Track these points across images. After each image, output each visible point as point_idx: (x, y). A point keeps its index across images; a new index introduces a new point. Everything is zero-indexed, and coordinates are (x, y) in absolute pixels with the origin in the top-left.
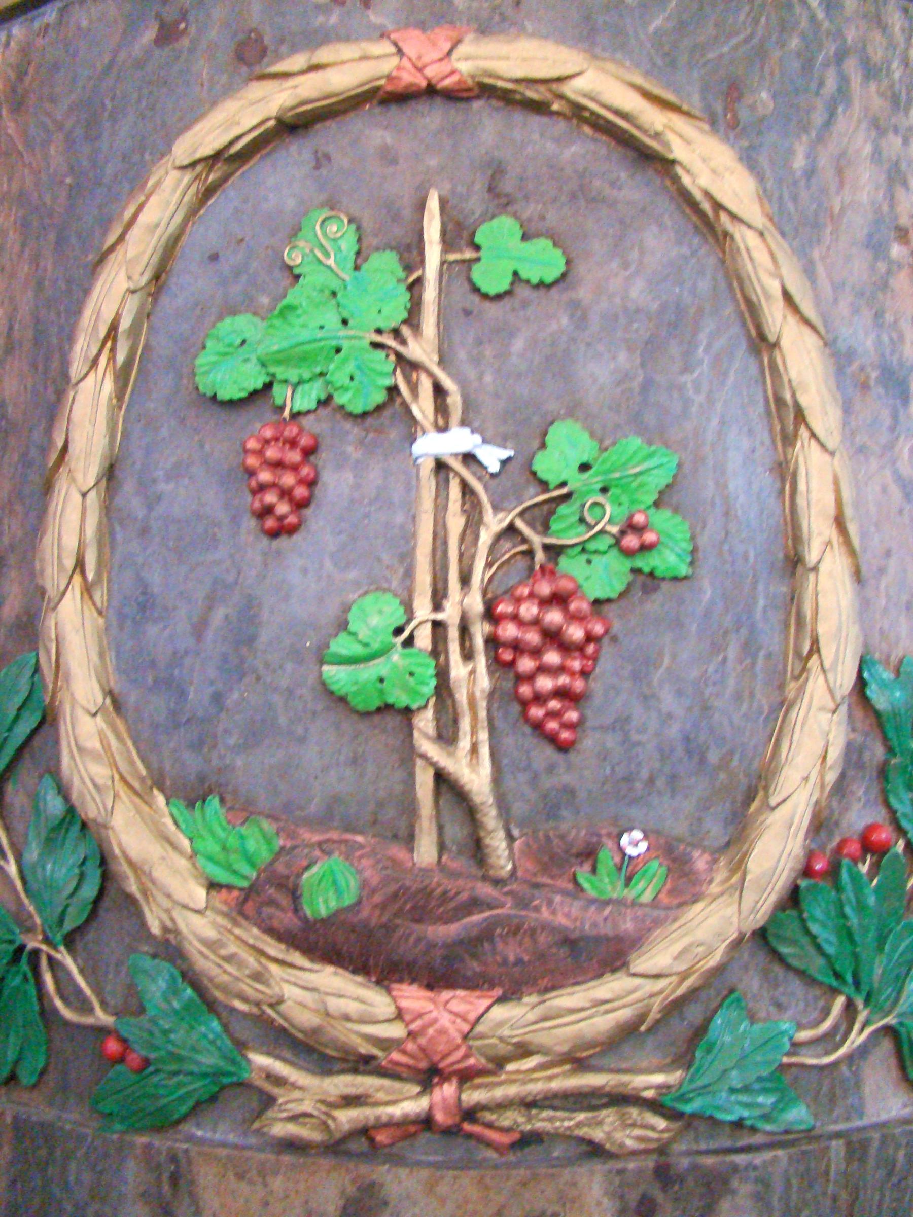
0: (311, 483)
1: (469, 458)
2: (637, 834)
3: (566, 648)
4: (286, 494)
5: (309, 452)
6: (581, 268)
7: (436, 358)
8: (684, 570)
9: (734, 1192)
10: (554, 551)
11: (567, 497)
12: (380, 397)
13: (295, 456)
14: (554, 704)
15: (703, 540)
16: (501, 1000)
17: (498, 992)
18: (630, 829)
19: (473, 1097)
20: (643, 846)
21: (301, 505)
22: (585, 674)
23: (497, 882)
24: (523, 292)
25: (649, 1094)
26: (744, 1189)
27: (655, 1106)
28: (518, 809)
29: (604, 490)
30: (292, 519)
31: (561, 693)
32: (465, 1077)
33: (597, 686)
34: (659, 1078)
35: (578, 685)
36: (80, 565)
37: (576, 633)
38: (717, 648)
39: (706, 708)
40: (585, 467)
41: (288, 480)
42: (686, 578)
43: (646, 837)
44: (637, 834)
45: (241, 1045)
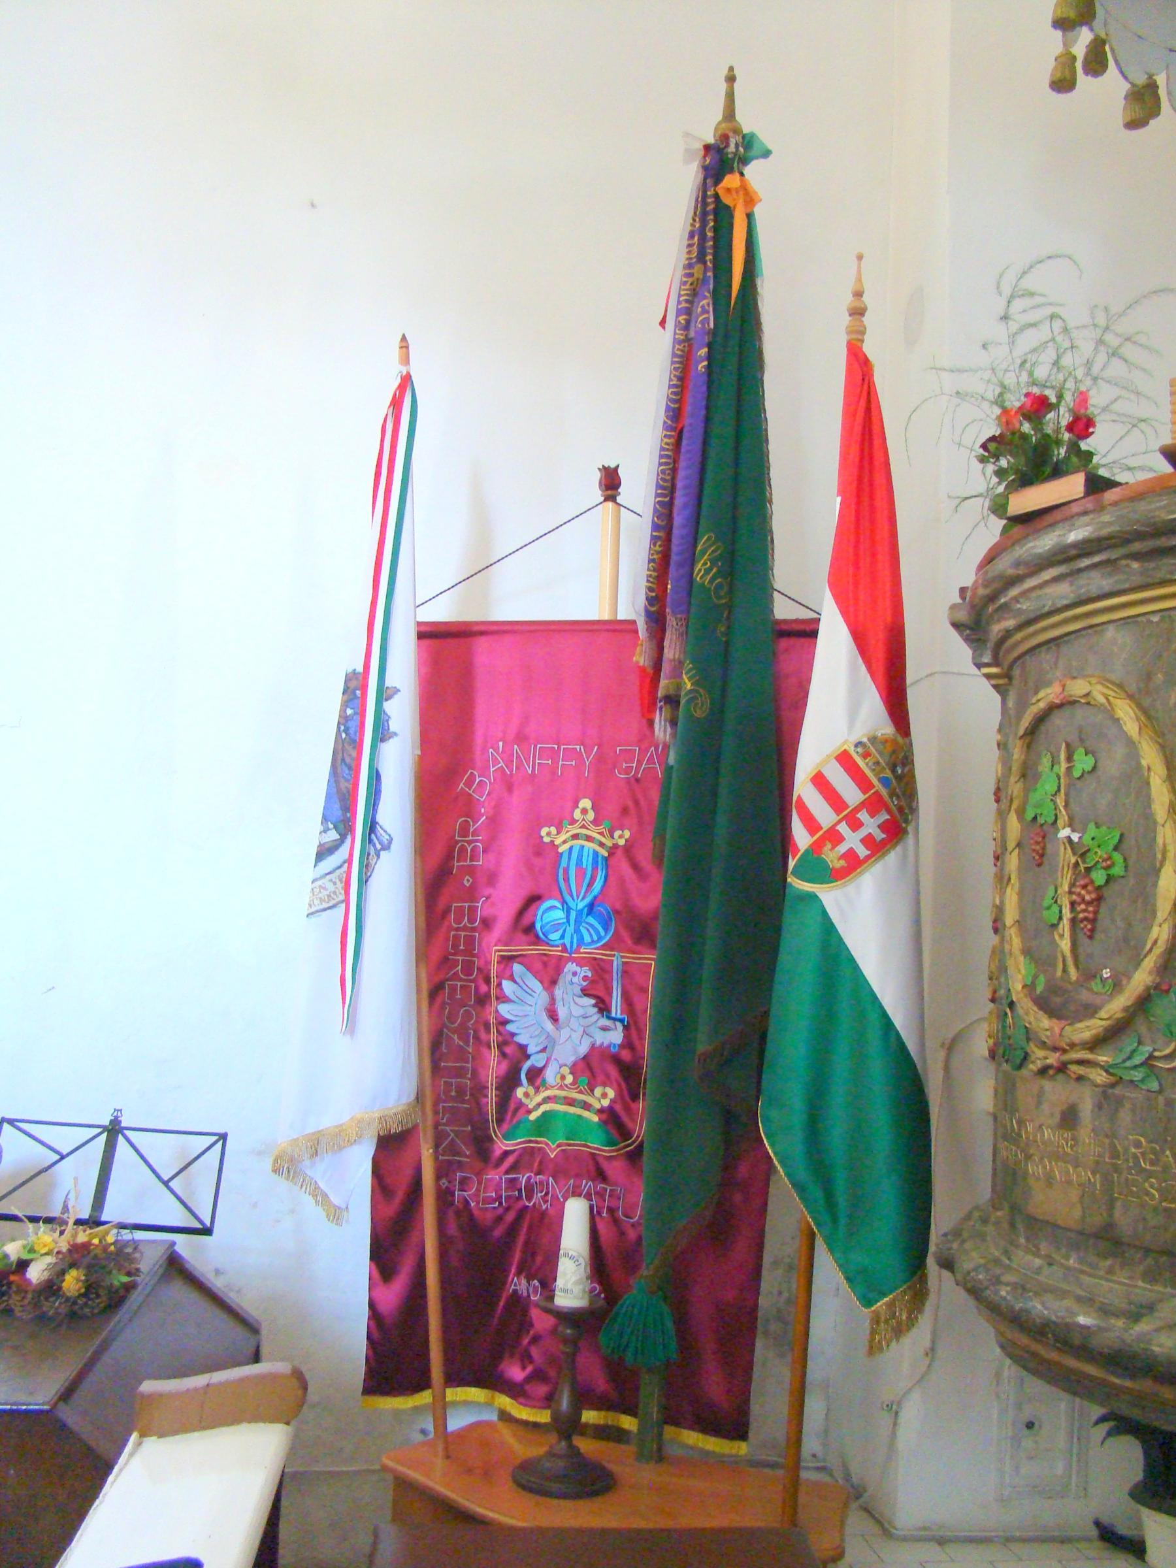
0: (1044, 848)
1: (1069, 838)
2: (1108, 970)
3: (1089, 903)
4: (1037, 853)
5: (1044, 837)
6: (1099, 764)
7: (1063, 804)
8: (1122, 873)
9: (1124, 1106)
10: (1088, 870)
11: (1089, 850)
12: (1054, 818)
13: (1040, 839)
14: (1085, 923)
15: (1131, 863)
16: (1069, 1024)
17: (1069, 1022)
18: (1106, 968)
19: (1066, 1057)
20: (1109, 974)
21: (1042, 856)
22: (1096, 913)
23: (1070, 983)
24: (1086, 775)
25: (1102, 1064)
26: (1128, 1105)
27: (1102, 1067)
28: (1082, 958)
29: (1099, 846)
30: (1040, 861)
31: (1085, 919)
32: (1064, 1051)
33: (1100, 916)
34: (1105, 1059)
35: (1091, 916)
36: (1009, 879)
37: (1088, 898)
38: (1135, 902)
39: (1130, 925)
40: (1093, 839)
41: (1038, 847)
42: (1123, 877)
43: (1110, 972)
44: (1108, 970)
45: (1028, 1039)
